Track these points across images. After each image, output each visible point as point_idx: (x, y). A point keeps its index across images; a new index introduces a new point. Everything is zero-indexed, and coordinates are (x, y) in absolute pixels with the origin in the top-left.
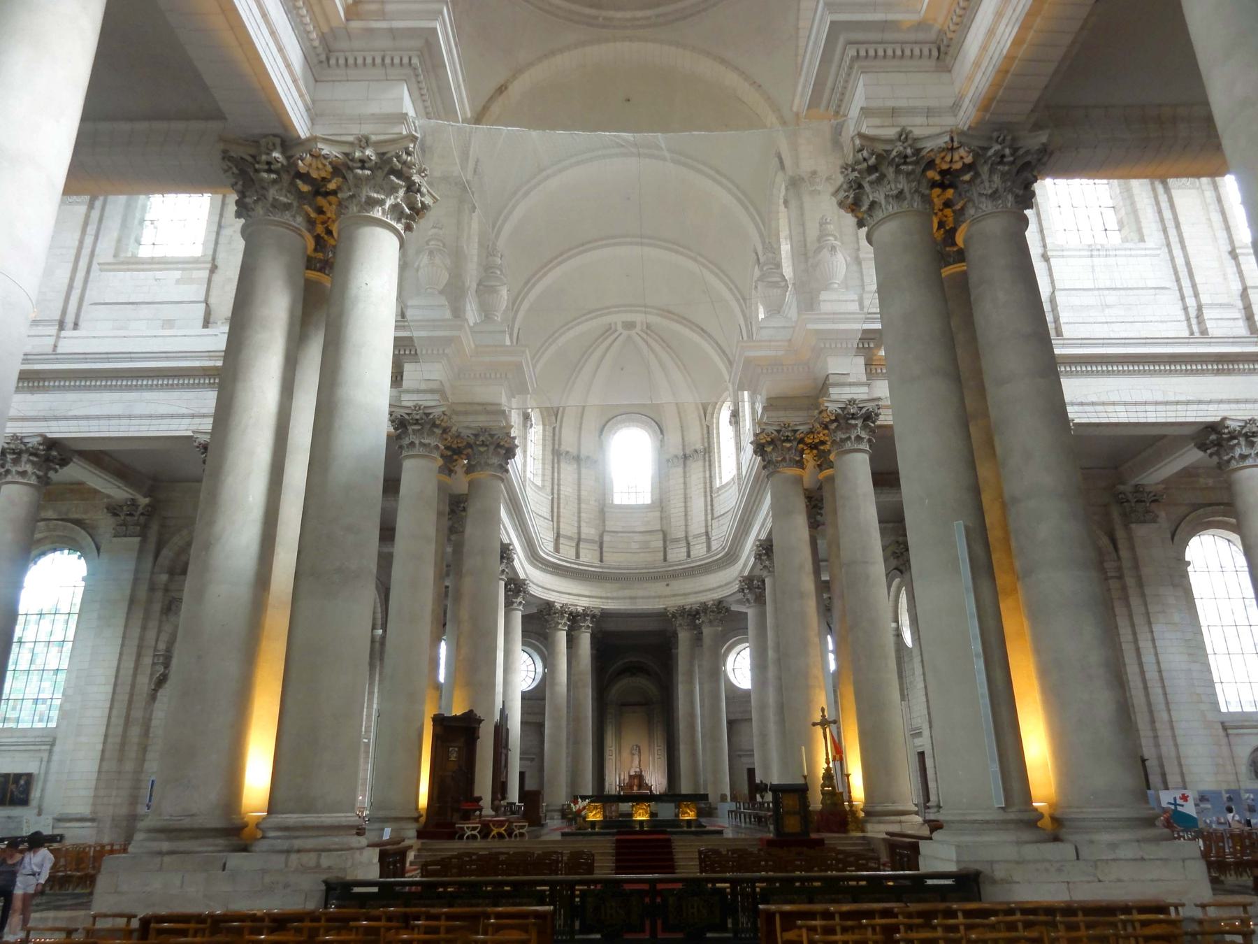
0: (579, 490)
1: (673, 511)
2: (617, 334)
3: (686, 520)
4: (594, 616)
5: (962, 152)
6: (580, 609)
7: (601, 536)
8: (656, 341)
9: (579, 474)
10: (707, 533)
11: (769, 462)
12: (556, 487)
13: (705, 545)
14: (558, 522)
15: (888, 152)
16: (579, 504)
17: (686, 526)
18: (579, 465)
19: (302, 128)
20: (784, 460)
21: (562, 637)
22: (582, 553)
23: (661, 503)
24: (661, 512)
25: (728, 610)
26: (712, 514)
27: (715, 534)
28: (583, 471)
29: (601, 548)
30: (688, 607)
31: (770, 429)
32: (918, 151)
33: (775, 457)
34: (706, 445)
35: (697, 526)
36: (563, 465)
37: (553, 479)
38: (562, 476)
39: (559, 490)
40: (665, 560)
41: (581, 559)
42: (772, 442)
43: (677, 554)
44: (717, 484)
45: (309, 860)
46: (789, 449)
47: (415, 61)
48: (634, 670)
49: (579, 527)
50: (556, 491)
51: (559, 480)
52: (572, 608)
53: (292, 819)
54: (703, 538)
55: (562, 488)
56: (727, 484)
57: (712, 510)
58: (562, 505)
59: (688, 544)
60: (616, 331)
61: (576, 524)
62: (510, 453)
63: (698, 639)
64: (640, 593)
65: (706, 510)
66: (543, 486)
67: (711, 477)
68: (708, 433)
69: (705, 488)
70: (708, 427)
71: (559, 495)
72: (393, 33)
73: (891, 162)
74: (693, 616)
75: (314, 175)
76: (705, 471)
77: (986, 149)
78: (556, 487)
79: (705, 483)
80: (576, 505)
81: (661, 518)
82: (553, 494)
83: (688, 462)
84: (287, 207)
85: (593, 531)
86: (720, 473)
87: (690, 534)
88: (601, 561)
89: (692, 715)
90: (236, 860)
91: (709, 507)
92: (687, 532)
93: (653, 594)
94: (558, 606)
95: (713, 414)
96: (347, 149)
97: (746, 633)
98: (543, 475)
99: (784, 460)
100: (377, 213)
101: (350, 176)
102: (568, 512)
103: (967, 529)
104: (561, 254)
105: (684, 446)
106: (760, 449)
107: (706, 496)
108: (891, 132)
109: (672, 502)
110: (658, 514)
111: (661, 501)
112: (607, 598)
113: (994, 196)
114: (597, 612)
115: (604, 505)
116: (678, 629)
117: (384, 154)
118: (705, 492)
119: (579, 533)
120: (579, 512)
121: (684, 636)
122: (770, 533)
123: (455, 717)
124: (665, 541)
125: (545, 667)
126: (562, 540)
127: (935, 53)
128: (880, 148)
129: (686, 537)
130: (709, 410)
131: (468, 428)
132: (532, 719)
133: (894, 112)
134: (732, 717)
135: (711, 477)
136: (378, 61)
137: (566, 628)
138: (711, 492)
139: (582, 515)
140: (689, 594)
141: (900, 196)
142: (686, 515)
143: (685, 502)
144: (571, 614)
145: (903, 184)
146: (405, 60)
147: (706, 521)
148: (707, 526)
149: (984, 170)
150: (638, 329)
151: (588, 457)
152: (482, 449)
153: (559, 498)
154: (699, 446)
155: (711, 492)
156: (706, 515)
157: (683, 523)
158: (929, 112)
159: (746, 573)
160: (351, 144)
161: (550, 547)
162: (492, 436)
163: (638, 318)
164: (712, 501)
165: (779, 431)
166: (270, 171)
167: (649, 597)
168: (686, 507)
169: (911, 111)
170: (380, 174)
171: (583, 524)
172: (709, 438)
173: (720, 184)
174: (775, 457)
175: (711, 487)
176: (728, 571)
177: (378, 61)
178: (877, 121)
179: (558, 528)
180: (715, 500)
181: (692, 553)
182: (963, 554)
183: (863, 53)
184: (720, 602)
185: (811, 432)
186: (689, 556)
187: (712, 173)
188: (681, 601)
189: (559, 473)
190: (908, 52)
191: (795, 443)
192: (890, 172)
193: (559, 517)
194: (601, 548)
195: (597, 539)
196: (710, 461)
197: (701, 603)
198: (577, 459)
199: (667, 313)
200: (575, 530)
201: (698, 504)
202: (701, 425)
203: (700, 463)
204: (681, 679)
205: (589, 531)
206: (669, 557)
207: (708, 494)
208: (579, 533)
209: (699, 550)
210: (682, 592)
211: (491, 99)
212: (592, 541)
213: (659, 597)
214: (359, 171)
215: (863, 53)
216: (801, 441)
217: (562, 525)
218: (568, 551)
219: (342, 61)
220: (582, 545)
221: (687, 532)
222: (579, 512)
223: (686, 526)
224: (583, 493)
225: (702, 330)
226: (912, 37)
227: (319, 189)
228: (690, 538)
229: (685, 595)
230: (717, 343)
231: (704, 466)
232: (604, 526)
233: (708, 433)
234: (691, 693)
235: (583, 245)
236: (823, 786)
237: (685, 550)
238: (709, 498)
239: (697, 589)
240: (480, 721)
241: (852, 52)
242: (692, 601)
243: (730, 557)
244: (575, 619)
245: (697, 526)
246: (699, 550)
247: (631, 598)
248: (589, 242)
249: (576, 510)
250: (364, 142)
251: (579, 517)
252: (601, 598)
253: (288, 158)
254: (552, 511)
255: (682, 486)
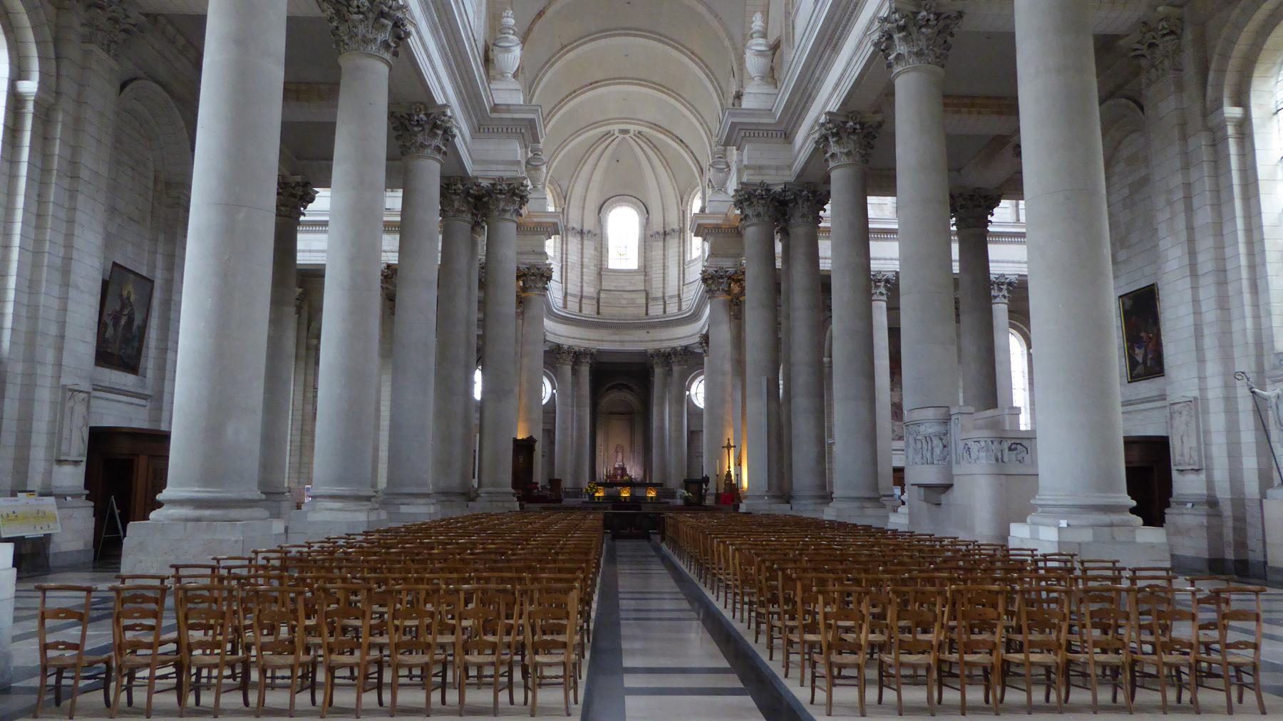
0: (582, 258)
1: (654, 275)
2: (614, 137)
3: (664, 284)
4: (592, 354)
5: (789, 193)
6: (582, 349)
7: (599, 293)
8: (646, 143)
9: (582, 245)
10: (679, 295)
11: (710, 290)
12: (564, 256)
13: (677, 304)
14: (566, 283)
15: (755, 191)
16: (582, 268)
17: (664, 288)
18: (582, 238)
19: (470, 168)
20: (718, 289)
21: (568, 369)
22: (583, 306)
23: (645, 269)
24: (645, 276)
25: (693, 353)
26: (684, 281)
27: (684, 297)
28: (586, 242)
29: (598, 303)
30: (663, 350)
31: (711, 270)
32: (768, 190)
33: (713, 287)
34: (682, 226)
35: (672, 289)
36: (570, 239)
37: (562, 250)
38: (569, 247)
39: (566, 258)
40: (647, 314)
41: (584, 312)
42: (712, 277)
43: (656, 310)
44: (688, 258)
45: (500, 504)
46: (722, 283)
47: (523, 131)
48: (620, 387)
49: (582, 287)
50: (564, 259)
51: (567, 250)
52: (577, 349)
53: (491, 489)
54: (676, 300)
55: (569, 256)
56: (696, 259)
57: (684, 278)
58: (569, 270)
59: (665, 302)
60: (613, 135)
61: (579, 284)
62: (549, 278)
63: (669, 373)
64: (627, 338)
65: (679, 278)
66: (555, 256)
67: (684, 251)
68: (683, 216)
69: (679, 260)
70: (683, 212)
71: (566, 262)
72: (513, 119)
73: (756, 197)
74: (667, 357)
75: (476, 193)
76: (679, 247)
77: (801, 191)
78: (564, 256)
79: (679, 256)
80: (580, 270)
81: (645, 281)
82: (562, 261)
83: (667, 238)
84: (463, 212)
85: (592, 290)
86: (691, 249)
87: (667, 295)
88: (598, 313)
89: (662, 428)
90: (471, 504)
91: (682, 275)
92: (664, 293)
93: (636, 339)
94: (566, 347)
95: (688, 201)
96: (492, 182)
97: (703, 368)
98: (555, 247)
99: (718, 289)
100: (508, 216)
101: (494, 195)
102: (573, 276)
103: (768, 380)
104: (575, 92)
105: (664, 224)
106: (704, 280)
107: (679, 267)
108: (757, 179)
109: (654, 269)
110: (642, 277)
111: (645, 267)
112: (602, 341)
113: (803, 216)
114: (594, 351)
115: (601, 269)
116: (655, 366)
117: (510, 184)
118: (679, 263)
119: (582, 292)
120: (582, 275)
121: (658, 371)
122: (708, 331)
123: (523, 440)
124: (647, 299)
125: (553, 388)
126: (569, 298)
127: (783, 136)
128: (750, 188)
129: (664, 297)
130: (685, 199)
131: (524, 264)
132: (548, 427)
133: (760, 168)
134: (692, 428)
135: (684, 251)
136: (505, 130)
137: (571, 363)
138: (684, 263)
139: (584, 277)
140: (665, 340)
141: (758, 215)
142: (664, 280)
143: (664, 269)
144: (575, 353)
145: (761, 209)
146: (518, 131)
147: (679, 286)
148: (679, 290)
149: (800, 201)
150: (631, 134)
151: (589, 232)
152: (533, 278)
153: (566, 265)
154: (676, 227)
155: (684, 263)
156: (679, 281)
157: (661, 286)
158: (777, 168)
159: (704, 332)
160: (494, 179)
161: (561, 305)
162: (539, 269)
163: (632, 128)
164: (684, 270)
165: (716, 272)
166: (455, 193)
167: (634, 341)
168: (664, 273)
169: (769, 167)
170: (509, 195)
171: (585, 284)
172: (684, 220)
173: (693, 60)
174: (713, 287)
175: (684, 260)
176: (693, 325)
177: (505, 130)
178: (751, 172)
179: (566, 288)
180: (686, 271)
181: (667, 310)
182: (765, 390)
183: (747, 134)
184: (686, 347)
185: (736, 273)
186: (665, 312)
187: (689, 53)
188: (657, 346)
189: (567, 244)
190: (770, 135)
191: (726, 279)
192: (755, 201)
193: (566, 279)
194: (598, 303)
195: (595, 295)
196: (684, 239)
197: (672, 348)
198: (582, 233)
199: (655, 126)
200: (579, 289)
201: (673, 272)
202: (679, 210)
203: (677, 240)
204: (655, 401)
205: (589, 290)
206: (650, 311)
207: (681, 264)
208: (582, 292)
209: (672, 308)
210: (659, 338)
211: (533, 23)
212: (594, 298)
213: (642, 341)
214: (499, 196)
215: (747, 134)
216: (729, 278)
217: (569, 286)
218: (573, 305)
219: (486, 130)
220: (584, 301)
221: (664, 293)
222: (582, 275)
223: (664, 288)
224: (586, 260)
225: (681, 141)
226: (772, 128)
227: (478, 198)
228: (666, 298)
229: (661, 340)
230: (692, 153)
231: (679, 243)
232: (601, 285)
233: (683, 216)
234: (662, 413)
235: (591, 84)
236: (726, 480)
237: (662, 307)
238: (682, 268)
239: (669, 337)
240: (535, 441)
241: (743, 134)
242: (665, 346)
243: (695, 317)
244: (577, 356)
245: (672, 289)
246: (672, 308)
247: (621, 341)
248: (597, 82)
249: (579, 274)
250: (501, 179)
251: (582, 279)
252: (598, 341)
253: (463, 185)
254: (562, 275)
255: (662, 257)
